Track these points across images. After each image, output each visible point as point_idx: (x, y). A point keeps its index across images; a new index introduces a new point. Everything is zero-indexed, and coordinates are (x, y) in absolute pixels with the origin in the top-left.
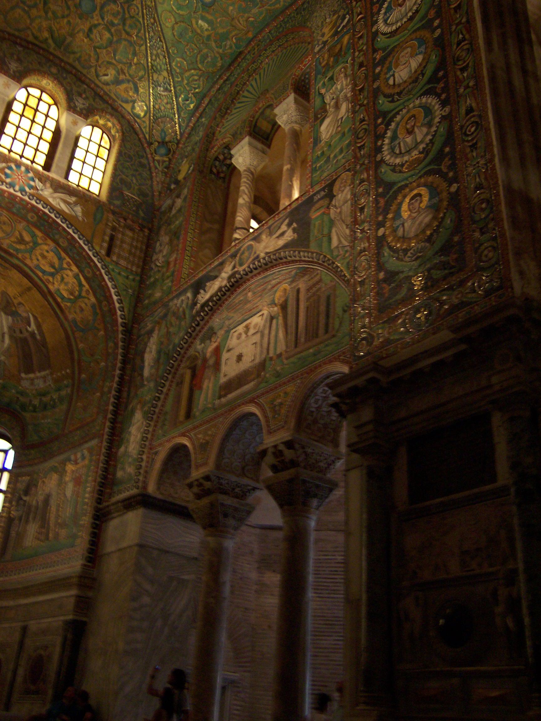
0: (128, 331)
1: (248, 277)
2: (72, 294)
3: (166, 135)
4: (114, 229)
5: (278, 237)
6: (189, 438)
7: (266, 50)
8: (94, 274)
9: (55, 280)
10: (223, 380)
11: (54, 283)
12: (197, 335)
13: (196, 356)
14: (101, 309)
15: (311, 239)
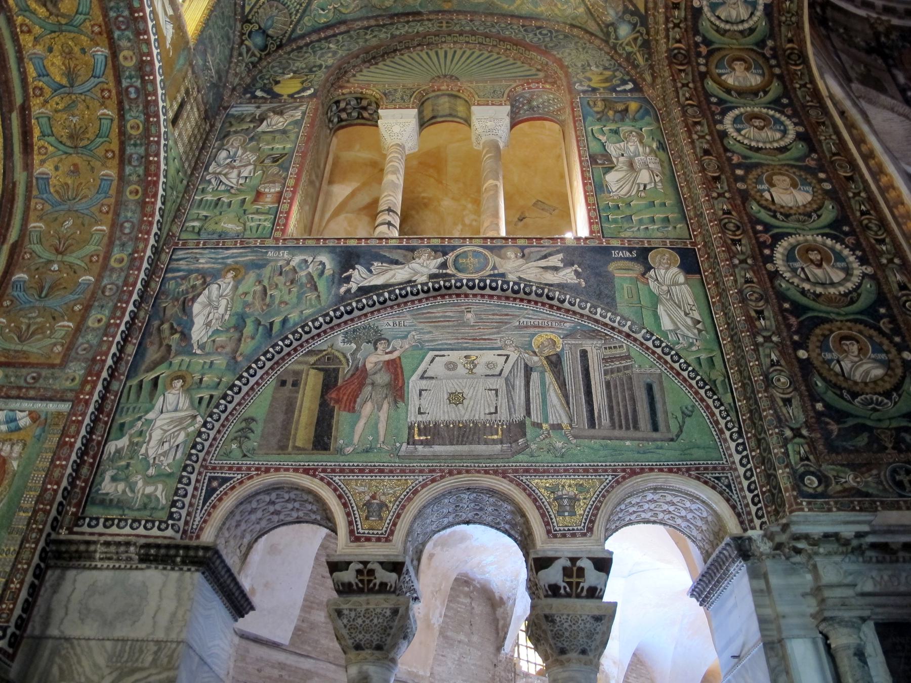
0: (157, 251)
1: (469, 291)
2: (71, 137)
3: (271, 26)
4: (187, 92)
5: (546, 268)
6: (329, 484)
7: (461, 35)
8: (147, 133)
9: (57, 99)
10: (413, 417)
11: (46, 102)
12: (339, 325)
13: (337, 357)
14: (120, 192)
15: (618, 300)
